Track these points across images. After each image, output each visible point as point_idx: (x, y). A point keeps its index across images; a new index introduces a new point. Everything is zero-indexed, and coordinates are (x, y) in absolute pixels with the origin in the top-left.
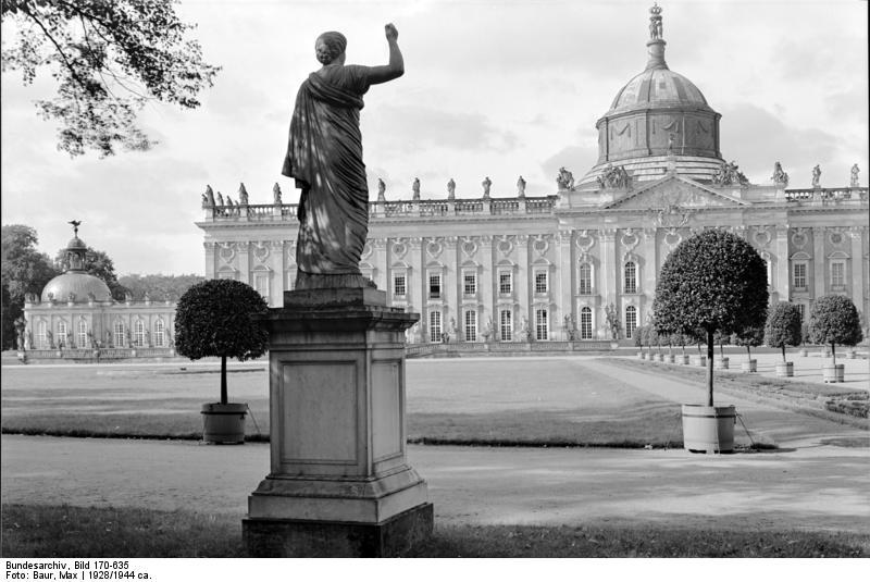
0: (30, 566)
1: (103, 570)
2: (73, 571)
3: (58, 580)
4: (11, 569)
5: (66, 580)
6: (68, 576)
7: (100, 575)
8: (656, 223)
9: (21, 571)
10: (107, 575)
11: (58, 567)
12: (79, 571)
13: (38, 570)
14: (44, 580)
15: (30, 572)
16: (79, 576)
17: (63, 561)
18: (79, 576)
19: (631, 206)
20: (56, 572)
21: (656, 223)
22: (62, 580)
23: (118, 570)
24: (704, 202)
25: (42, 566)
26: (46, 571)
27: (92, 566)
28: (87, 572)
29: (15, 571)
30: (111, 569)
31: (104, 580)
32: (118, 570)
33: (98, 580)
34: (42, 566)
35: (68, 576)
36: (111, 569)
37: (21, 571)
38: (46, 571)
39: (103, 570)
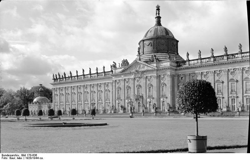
0: (9, 155)
1: (30, 156)
2: (21, 157)
3: (17, 159)
5: (19, 159)
6: (20, 158)
7: (29, 158)
8: (133, 77)
9: (6, 157)
10: (31, 158)
11: (17, 156)
12: (23, 157)
14: (13, 159)
16: (23, 158)
17: (18, 154)
18: (23, 158)
19: (128, 72)
20: (16, 157)
21: (133, 77)
22: (18, 159)
23: (34, 157)
24: (146, 68)
25: (12, 156)
26: (13, 157)
27: (26, 155)
28: (25, 157)
29: (4, 157)
30: (32, 156)
31: (30, 159)
32: (34, 157)
33: (28, 159)
34: (12, 156)
35: (20, 158)
36: (32, 156)
37: (6, 157)
38: (13, 157)
39: (30, 156)
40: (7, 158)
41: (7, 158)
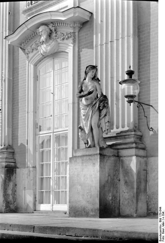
0: (160, 235)
2: (162, 223)
4: (162, 240)
6: (163, 224)
9: (162, 237)
12: (162, 221)
13: (162, 232)
15: (162, 235)
16: (163, 221)
18: (163, 221)
20: (162, 227)
25: (161, 231)
26: (162, 230)
27: (160, 217)
28: (162, 219)
29: (162, 239)
34: (161, 231)
35: (163, 224)
37: (162, 237)
38: (162, 230)
40: (163, 237)
41: (163, 237)
